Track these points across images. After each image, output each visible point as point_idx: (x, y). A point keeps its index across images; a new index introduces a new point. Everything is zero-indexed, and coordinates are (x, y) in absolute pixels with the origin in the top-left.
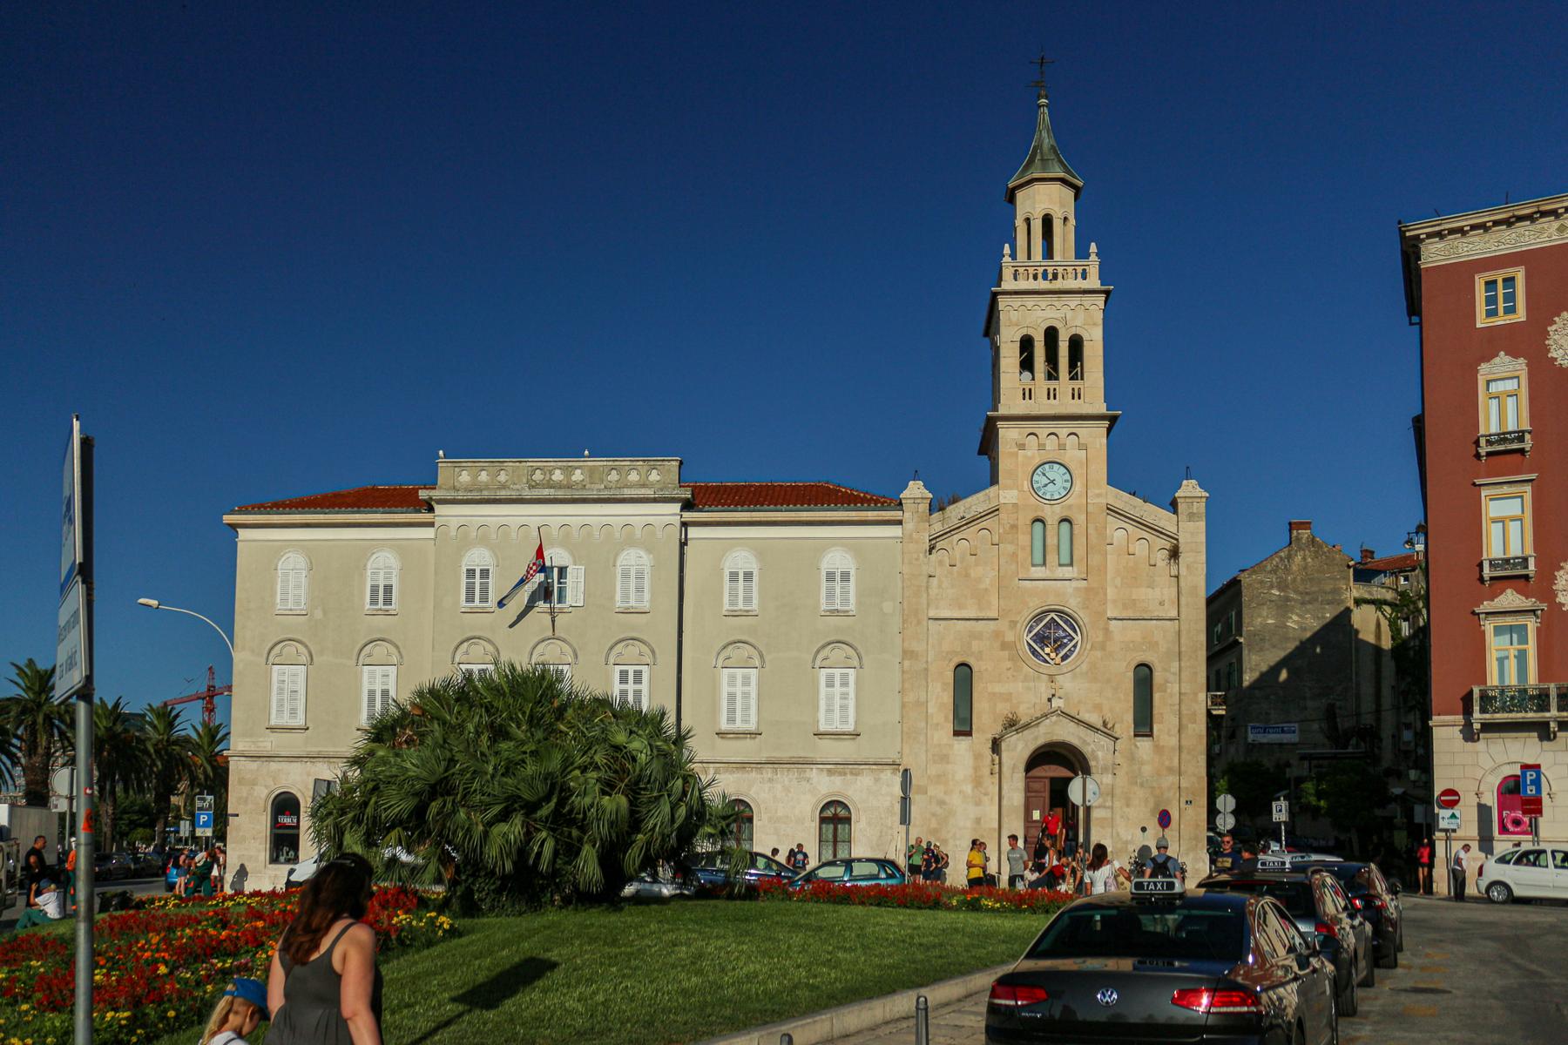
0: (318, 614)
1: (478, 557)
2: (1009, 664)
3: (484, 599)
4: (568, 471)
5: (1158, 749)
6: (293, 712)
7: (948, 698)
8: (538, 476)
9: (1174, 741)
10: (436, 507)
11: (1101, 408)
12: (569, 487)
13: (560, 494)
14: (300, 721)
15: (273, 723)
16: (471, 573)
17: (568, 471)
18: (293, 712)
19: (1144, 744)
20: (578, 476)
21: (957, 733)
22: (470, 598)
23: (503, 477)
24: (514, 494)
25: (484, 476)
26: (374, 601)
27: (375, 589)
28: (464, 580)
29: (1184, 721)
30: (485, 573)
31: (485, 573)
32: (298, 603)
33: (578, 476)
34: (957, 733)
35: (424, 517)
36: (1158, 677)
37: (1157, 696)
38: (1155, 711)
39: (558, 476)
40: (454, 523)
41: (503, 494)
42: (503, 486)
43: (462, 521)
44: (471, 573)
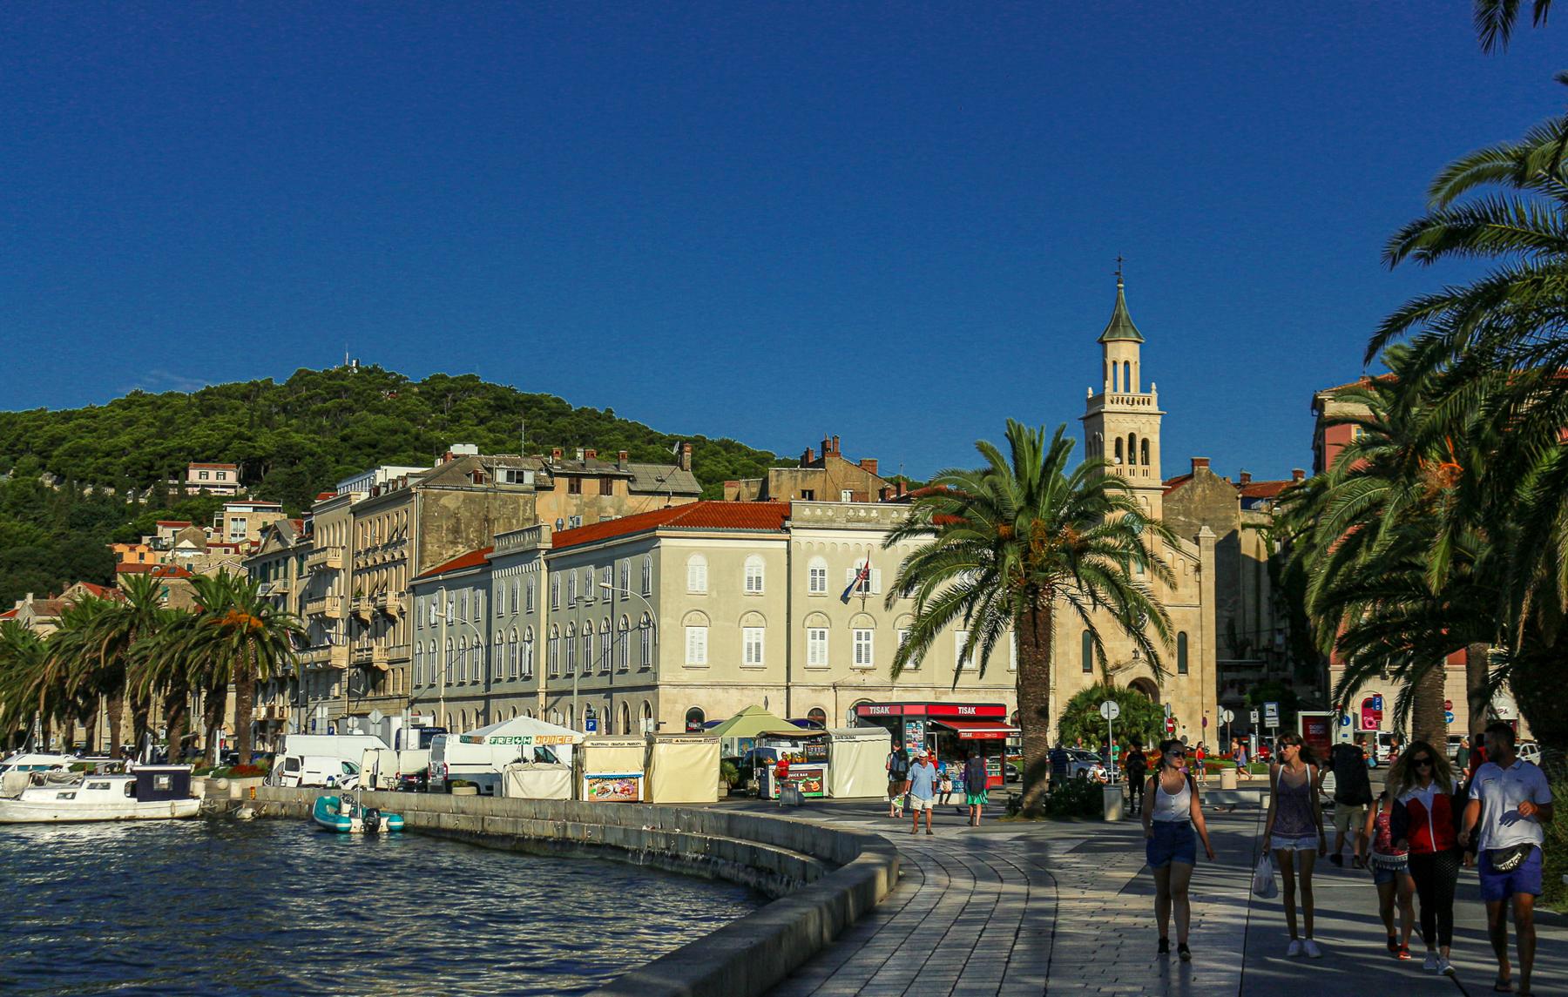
0: (714, 594)
1: (818, 562)
2: (1112, 631)
3: (822, 588)
4: (868, 511)
5: (1191, 681)
6: (700, 657)
7: (1079, 650)
8: (851, 513)
9: (1199, 677)
10: (792, 530)
11: (1159, 483)
12: (869, 521)
13: (861, 525)
14: (704, 662)
15: (687, 664)
16: (814, 572)
17: (868, 511)
18: (700, 657)
19: (1183, 677)
20: (874, 514)
21: (1084, 671)
22: (814, 588)
23: (830, 513)
24: (843, 526)
25: (819, 512)
26: (750, 587)
27: (750, 579)
28: (810, 577)
29: (1204, 665)
30: (822, 572)
31: (822, 572)
32: (702, 587)
33: (874, 514)
34: (1084, 671)
35: (786, 536)
36: (1190, 639)
37: (1190, 650)
38: (1189, 659)
39: (862, 513)
40: (803, 541)
41: (835, 525)
42: (831, 520)
43: (809, 539)
44: (814, 572)
